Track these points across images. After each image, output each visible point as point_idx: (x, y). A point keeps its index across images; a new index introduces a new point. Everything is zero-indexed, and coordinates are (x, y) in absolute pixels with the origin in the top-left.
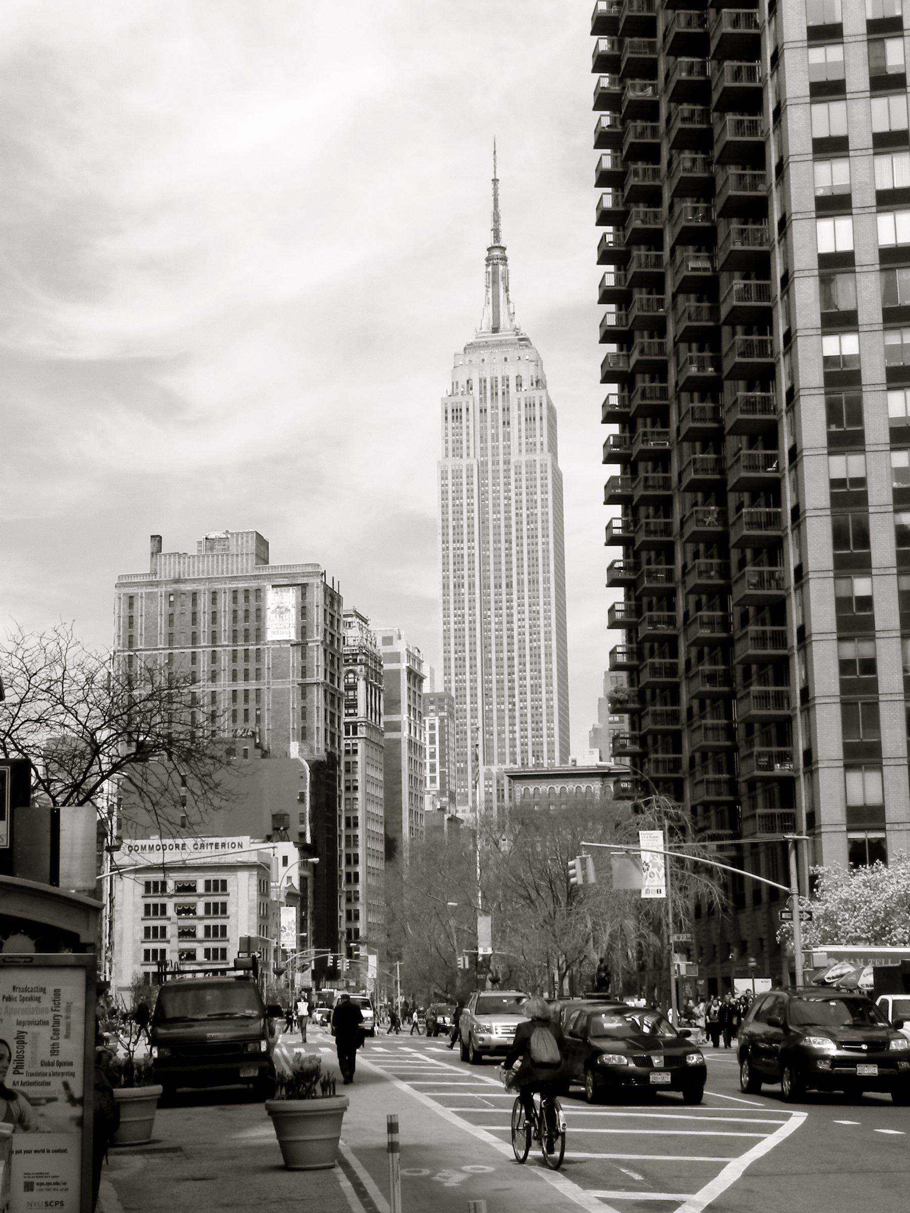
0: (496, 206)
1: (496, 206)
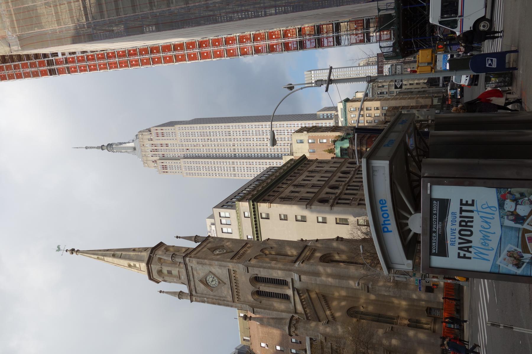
0: (94, 148)
1: (94, 148)
